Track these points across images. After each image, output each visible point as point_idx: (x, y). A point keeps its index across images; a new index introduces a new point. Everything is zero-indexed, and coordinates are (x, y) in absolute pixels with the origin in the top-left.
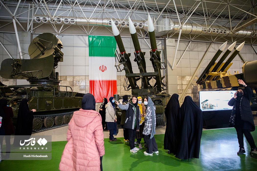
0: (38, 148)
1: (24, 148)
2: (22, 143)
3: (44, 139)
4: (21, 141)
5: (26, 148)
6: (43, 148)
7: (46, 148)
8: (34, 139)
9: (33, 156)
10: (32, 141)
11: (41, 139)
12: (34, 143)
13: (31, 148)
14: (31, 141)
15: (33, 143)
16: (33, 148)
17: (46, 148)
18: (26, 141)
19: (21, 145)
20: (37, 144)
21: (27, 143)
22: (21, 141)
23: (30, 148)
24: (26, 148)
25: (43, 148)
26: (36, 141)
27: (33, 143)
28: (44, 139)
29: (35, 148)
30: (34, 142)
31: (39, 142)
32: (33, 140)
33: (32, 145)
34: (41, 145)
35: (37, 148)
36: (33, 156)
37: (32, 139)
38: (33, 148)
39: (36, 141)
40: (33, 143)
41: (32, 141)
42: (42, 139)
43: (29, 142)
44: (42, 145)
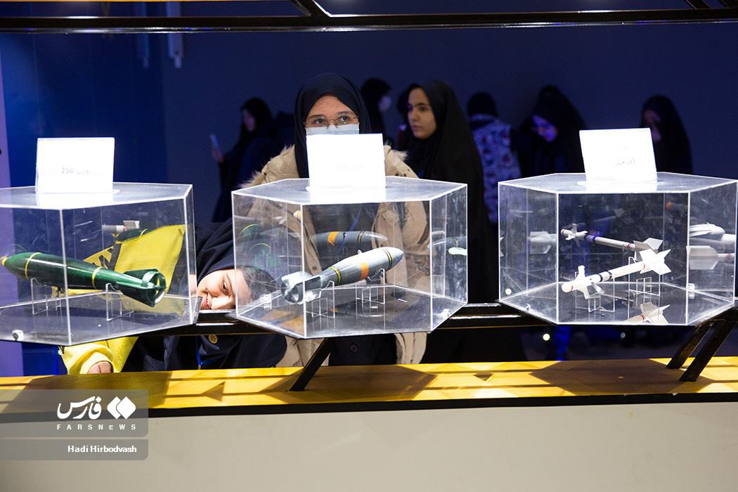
0: (110, 427)
1: (69, 427)
2: (63, 412)
3: (126, 399)
4: (60, 404)
5: (74, 427)
6: (122, 427)
7: (133, 427)
8: (99, 399)
9: (93, 447)
10: (92, 404)
11: (117, 400)
12: (97, 413)
13: (90, 427)
14: (88, 405)
15: (94, 413)
16: (95, 427)
17: (133, 427)
18: (74, 405)
19: (61, 416)
20: (106, 415)
21: (77, 411)
22: (60, 404)
23: (85, 427)
24: (74, 427)
25: (122, 427)
26: (104, 404)
27: (95, 410)
28: (126, 399)
29: (101, 427)
30: (98, 408)
31: (111, 408)
32: (95, 402)
33: (92, 416)
34: (117, 416)
35: (106, 427)
36: (93, 447)
37: (92, 399)
38: (95, 427)
39: (104, 404)
40: (94, 413)
41: (92, 404)
42: (121, 399)
43: (83, 408)
44: (121, 417)
